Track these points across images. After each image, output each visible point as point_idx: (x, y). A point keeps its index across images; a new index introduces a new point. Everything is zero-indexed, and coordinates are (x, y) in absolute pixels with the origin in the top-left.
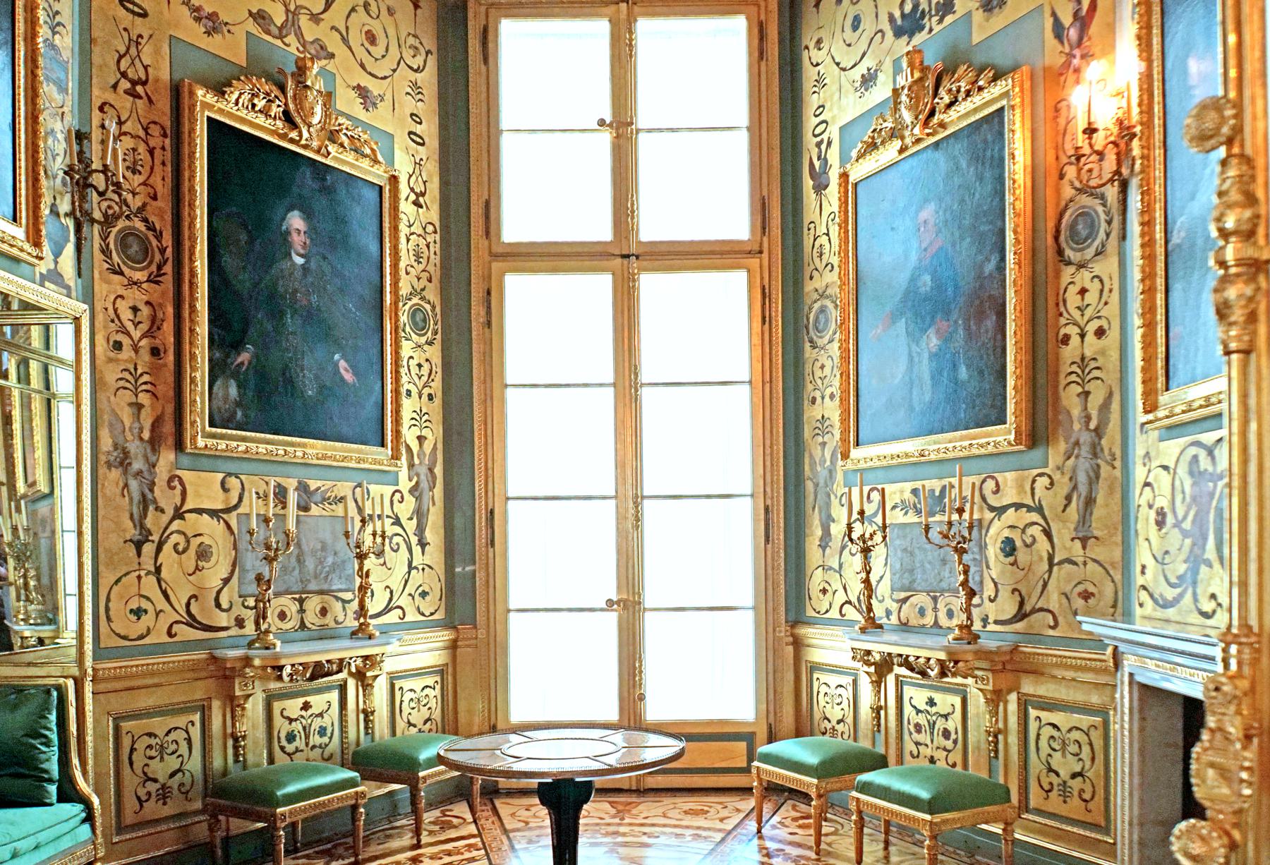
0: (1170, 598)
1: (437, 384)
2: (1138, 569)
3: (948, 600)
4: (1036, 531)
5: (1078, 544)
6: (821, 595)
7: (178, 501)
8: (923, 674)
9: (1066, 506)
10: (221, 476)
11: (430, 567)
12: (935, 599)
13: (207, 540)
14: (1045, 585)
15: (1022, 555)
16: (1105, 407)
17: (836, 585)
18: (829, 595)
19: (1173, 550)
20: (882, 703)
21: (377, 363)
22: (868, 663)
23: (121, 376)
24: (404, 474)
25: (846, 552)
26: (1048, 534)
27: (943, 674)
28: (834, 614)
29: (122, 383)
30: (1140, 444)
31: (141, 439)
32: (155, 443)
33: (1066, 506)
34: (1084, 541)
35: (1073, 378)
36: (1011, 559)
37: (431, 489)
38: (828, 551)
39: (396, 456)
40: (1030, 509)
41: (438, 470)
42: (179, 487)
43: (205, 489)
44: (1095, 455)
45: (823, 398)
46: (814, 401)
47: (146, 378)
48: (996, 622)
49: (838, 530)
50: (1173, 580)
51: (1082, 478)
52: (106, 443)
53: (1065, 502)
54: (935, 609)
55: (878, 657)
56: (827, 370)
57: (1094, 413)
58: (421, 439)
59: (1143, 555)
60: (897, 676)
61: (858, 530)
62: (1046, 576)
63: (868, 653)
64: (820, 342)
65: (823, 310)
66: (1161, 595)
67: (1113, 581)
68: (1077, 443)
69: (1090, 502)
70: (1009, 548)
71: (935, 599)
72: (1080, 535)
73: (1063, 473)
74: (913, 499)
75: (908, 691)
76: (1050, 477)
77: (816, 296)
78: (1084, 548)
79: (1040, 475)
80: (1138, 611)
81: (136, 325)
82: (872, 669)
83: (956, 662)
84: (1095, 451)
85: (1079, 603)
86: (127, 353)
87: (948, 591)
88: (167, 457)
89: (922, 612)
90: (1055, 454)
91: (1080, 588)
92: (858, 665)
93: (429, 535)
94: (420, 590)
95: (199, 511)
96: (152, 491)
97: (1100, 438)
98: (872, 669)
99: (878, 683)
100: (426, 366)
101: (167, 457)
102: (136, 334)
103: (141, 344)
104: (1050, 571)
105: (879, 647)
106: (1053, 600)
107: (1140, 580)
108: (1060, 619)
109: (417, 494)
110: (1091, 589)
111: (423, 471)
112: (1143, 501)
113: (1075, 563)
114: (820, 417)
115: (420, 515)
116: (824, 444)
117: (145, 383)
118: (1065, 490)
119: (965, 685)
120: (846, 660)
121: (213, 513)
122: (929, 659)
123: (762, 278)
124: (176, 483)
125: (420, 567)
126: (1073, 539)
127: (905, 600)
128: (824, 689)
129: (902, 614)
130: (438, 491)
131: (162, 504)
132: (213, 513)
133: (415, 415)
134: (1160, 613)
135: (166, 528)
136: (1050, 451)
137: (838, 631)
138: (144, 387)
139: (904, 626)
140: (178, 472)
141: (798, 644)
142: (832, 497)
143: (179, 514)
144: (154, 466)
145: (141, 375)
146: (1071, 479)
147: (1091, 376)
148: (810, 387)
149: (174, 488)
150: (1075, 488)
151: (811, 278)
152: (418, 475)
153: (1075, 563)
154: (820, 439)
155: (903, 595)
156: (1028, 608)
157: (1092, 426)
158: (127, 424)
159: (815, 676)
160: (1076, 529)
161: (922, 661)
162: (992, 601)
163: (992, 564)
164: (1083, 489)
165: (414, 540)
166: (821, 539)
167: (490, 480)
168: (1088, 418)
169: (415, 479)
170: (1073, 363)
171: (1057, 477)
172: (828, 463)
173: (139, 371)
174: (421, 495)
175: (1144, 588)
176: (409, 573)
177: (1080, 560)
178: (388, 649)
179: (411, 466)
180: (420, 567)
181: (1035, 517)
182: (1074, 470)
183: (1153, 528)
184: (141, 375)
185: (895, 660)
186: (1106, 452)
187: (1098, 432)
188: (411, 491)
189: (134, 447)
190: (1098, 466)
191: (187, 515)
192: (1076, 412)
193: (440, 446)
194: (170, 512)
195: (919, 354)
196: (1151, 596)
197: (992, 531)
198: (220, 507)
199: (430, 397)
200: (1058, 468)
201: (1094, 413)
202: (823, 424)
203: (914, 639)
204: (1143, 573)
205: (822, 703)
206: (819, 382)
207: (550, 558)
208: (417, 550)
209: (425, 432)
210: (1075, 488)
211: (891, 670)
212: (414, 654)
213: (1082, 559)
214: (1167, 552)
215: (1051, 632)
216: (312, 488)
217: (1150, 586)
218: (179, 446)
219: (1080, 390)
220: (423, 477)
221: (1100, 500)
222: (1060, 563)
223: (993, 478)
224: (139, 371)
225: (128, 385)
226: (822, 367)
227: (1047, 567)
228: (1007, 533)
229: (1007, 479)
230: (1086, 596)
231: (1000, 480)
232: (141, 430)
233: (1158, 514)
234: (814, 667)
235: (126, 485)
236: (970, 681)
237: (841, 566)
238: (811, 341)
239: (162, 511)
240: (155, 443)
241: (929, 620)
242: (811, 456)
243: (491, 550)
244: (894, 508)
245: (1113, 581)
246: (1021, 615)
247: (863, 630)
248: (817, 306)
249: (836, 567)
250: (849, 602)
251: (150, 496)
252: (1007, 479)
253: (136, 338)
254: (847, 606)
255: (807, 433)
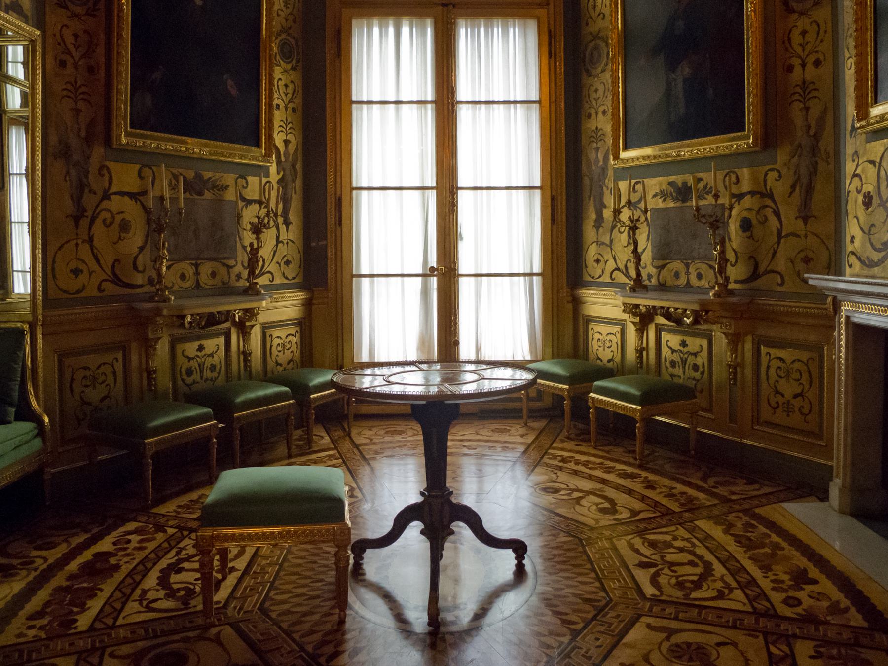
0: (876, 260)
1: (299, 100)
2: (848, 239)
3: (698, 265)
4: (769, 212)
5: (800, 222)
6: (595, 264)
7: (107, 184)
8: (679, 321)
9: (791, 193)
10: (138, 167)
11: (292, 242)
12: (687, 266)
13: (128, 217)
14: (775, 252)
15: (757, 231)
16: (822, 119)
17: (608, 256)
18: (602, 264)
19: (877, 224)
20: (645, 345)
21: (252, 84)
22: (635, 315)
23: (65, 87)
24: (273, 169)
25: (616, 231)
26: (777, 214)
27: (696, 322)
28: (606, 278)
29: (65, 93)
30: (849, 147)
31: (79, 136)
32: (89, 140)
33: (791, 193)
34: (805, 219)
35: (796, 97)
36: (748, 234)
37: (294, 181)
38: (601, 230)
39: (268, 155)
40: (763, 195)
41: (299, 166)
42: (107, 175)
43: (126, 177)
44: (814, 155)
45: (597, 114)
46: (589, 116)
47: (83, 89)
48: (736, 282)
49: (608, 214)
50: (879, 246)
51: (803, 171)
52: (54, 139)
53: (790, 190)
54: (688, 273)
55: (643, 310)
56: (600, 93)
57: (813, 124)
58: (286, 142)
59: (853, 229)
60: (657, 325)
61: (625, 214)
62: (776, 246)
63: (637, 306)
64: (594, 72)
65: (596, 48)
66: (868, 258)
67: (828, 248)
68: (800, 145)
69: (809, 190)
70: (746, 225)
71: (687, 266)
72: (803, 214)
73: (789, 168)
74: (671, 189)
75: (666, 336)
76: (779, 171)
77: (591, 38)
78: (805, 224)
79: (772, 170)
80: (848, 270)
81: (77, 48)
82: (637, 320)
83: (707, 312)
84: (814, 150)
85: (801, 266)
86: (70, 70)
87: (698, 259)
88: (98, 151)
89: (677, 275)
90: (782, 156)
91: (802, 255)
92: (625, 316)
93: (292, 216)
94: (285, 259)
95: (122, 194)
96: (87, 177)
97: (818, 142)
98: (637, 320)
99: (641, 329)
100: (291, 86)
101: (98, 151)
102: (77, 55)
103: (80, 63)
104: (779, 243)
105: (645, 302)
106: (781, 264)
107: (849, 248)
108: (786, 278)
109: (283, 184)
110: (811, 255)
111: (288, 166)
112: (852, 188)
113: (798, 236)
114: (594, 128)
115: (285, 200)
116: (597, 149)
117: (83, 93)
118: (790, 182)
119: (711, 330)
120: (617, 313)
121: (132, 196)
122: (686, 310)
123: (549, 24)
124: (105, 171)
125: (285, 242)
126: (796, 218)
127: (663, 267)
128: (597, 336)
129: (661, 277)
130: (298, 183)
131: (95, 187)
132: (132, 196)
133: (282, 124)
134: (866, 271)
135: (97, 206)
136: (779, 152)
137: (611, 291)
138: (82, 96)
139: (662, 287)
140: (107, 163)
141: (577, 302)
142: (605, 188)
143: (106, 196)
144: (88, 158)
145: (80, 87)
146: (795, 172)
147: (811, 95)
148: (586, 105)
149: (103, 175)
150: (799, 178)
151: (587, 24)
152: (284, 170)
153: (798, 236)
154: (595, 145)
155: (661, 263)
156: (762, 269)
157: (812, 133)
158: (69, 124)
159: (590, 327)
160: (799, 211)
161: (680, 311)
162: (732, 266)
163: (733, 236)
164: (804, 180)
165: (280, 220)
166: (596, 221)
167: (339, 174)
168: (809, 127)
169: (282, 173)
170: (797, 86)
171: (784, 172)
172: (601, 163)
173: (78, 85)
174: (286, 185)
175: (853, 253)
176: (277, 245)
177: (802, 233)
178: (264, 303)
179: (279, 162)
180: (285, 242)
181: (768, 202)
182: (798, 166)
183: (861, 211)
184: (80, 87)
185: (658, 312)
186: (822, 152)
187: (817, 137)
188: (279, 182)
189: (74, 141)
190: (817, 163)
191: (113, 197)
192: (799, 121)
193: (300, 147)
194: (100, 194)
195: (675, 80)
196: (859, 259)
197: (734, 212)
198: (136, 191)
199: (294, 110)
200: (785, 164)
201: (813, 124)
202: (597, 135)
203: (671, 296)
204: (852, 241)
205: (596, 347)
206: (594, 102)
207: (387, 235)
208: (283, 228)
209: (290, 137)
210: (799, 178)
211: (651, 320)
212: (283, 307)
213: (803, 233)
214: (873, 225)
215: (779, 289)
216: (206, 178)
217: (859, 251)
218: (108, 141)
219: (802, 105)
220: (288, 172)
221: (818, 187)
222: (787, 236)
223: (734, 172)
224: (78, 85)
225: (70, 94)
226: (596, 91)
227: (776, 239)
228: (745, 214)
229: (745, 173)
230: (807, 260)
231: (739, 174)
232: (80, 129)
233: (865, 196)
234: (588, 320)
235: (68, 173)
236: (714, 327)
237: (611, 241)
238: (587, 71)
239: (95, 193)
240: (89, 140)
241: (683, 281)
242: (588, 160)
243: (339, 229)
244: (654, 196)
245: (828, 248)
246: (755, 276)
247: (633, 289)
248: (592, 45)
249: (608, 243)
250: (618, 269)
251: (85, 180)
252: (745, 173)
253: (77, 59)
254: (616, 272)
255: (584, 141)
